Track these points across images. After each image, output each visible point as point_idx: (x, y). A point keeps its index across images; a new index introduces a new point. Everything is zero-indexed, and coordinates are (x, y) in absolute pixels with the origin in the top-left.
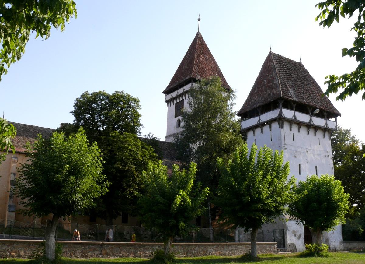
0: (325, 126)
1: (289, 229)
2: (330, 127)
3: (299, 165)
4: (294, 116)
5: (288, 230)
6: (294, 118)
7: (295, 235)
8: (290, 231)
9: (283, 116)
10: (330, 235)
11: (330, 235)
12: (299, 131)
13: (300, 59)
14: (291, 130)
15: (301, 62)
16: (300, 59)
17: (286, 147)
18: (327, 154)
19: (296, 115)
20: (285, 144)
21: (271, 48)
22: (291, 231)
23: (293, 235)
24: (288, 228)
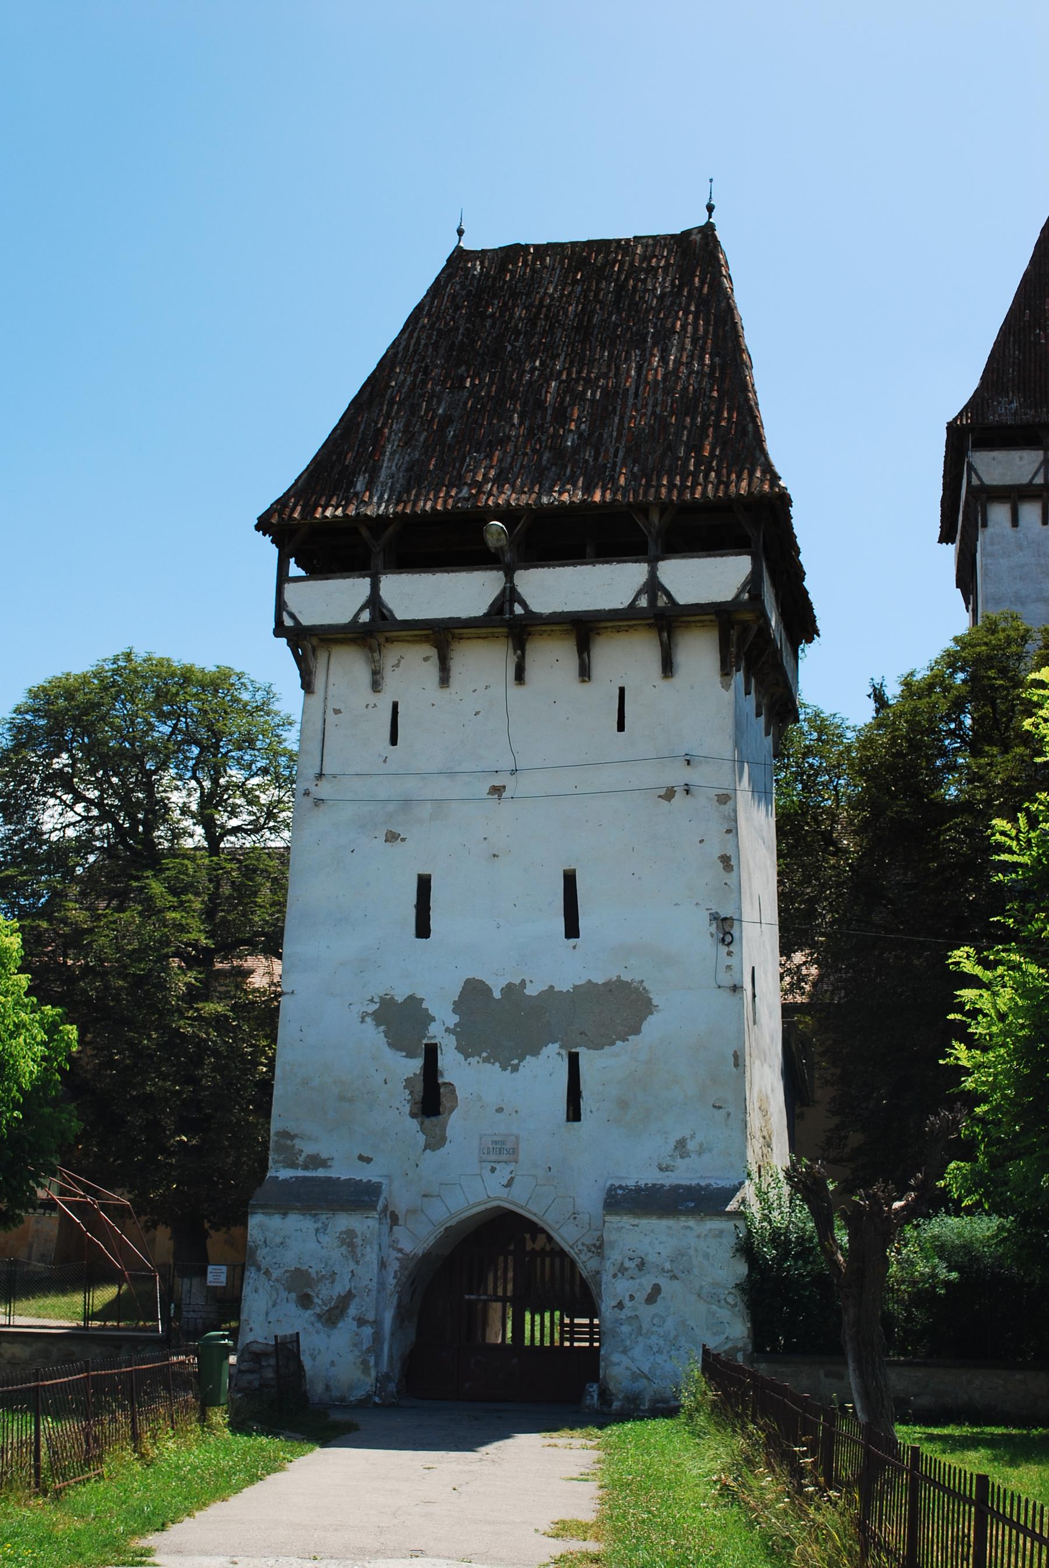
0: (643, 602)
1: (264, 1265)
2: (682, 600)
3: (424, 885)
4: (374, 602)
5: (259, 1269)
6: (365, 617)
7: (305, 1301)
8: (267, 1273)
9: (288, 622)
10: (620, 1306)
11: (620, 1306)
12: (445, 680)
13: (710, 208)
14: (376, 686)
15: (708, 230)
16: (710, 208)
17: (324, 790)
18: (677, 775)
19: (383, 593)
20: (320, 775)
21: (460, 232)
22: (276, 1274)
23: (293, 1296)
24: (261, 1253)
